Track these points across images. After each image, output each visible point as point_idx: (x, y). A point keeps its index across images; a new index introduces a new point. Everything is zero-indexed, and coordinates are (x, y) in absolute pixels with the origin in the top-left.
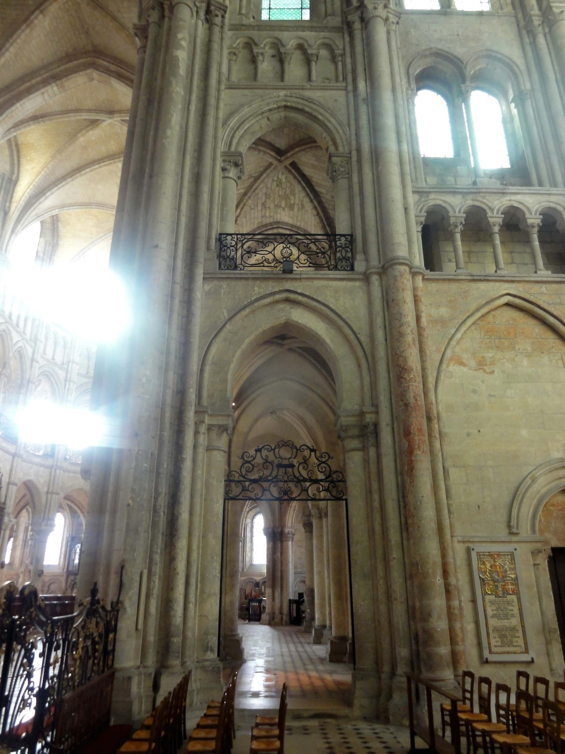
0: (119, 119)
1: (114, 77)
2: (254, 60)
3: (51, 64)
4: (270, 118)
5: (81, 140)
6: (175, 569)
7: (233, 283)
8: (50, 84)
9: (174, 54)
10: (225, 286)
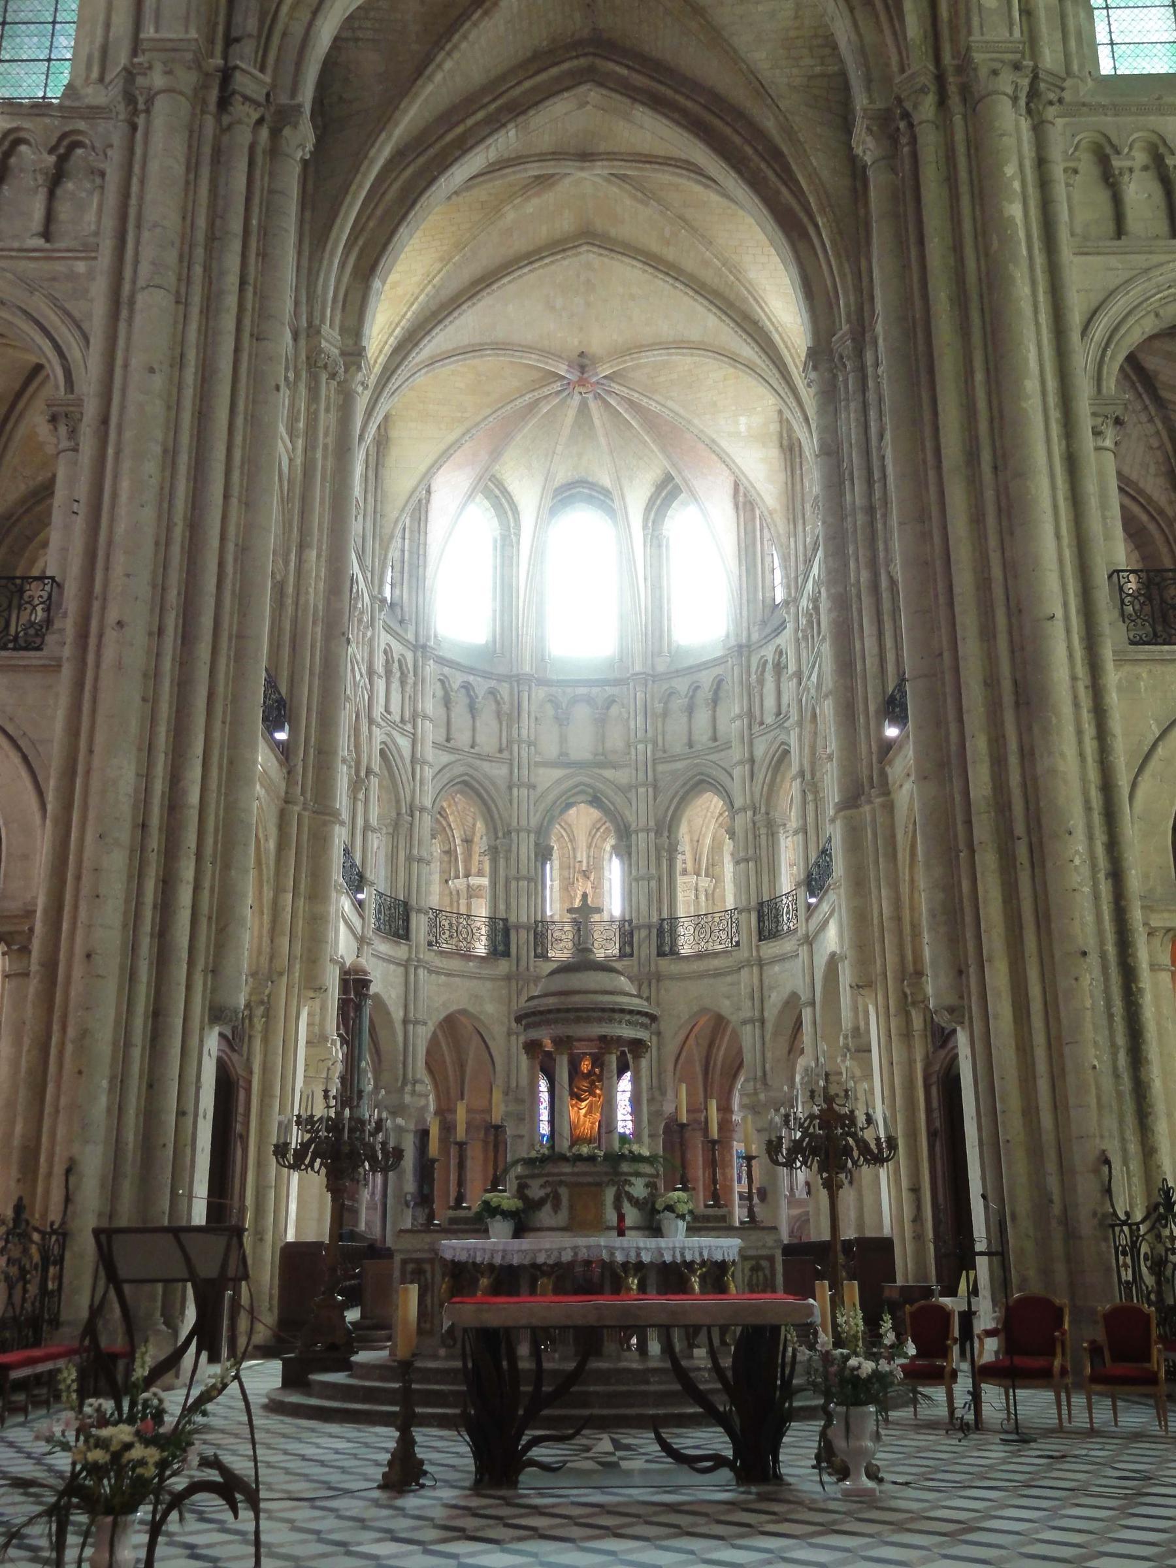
0: (606, 172)
1: (643, 103)
2: (1110, 181)
3: (503, 77)
4: (1161, 312)
5: (510, 215)
6: (1159, 1167)
7: (1158, 669)
8: (504, 125)
9: (1006, 215)
10: (1144, 675)
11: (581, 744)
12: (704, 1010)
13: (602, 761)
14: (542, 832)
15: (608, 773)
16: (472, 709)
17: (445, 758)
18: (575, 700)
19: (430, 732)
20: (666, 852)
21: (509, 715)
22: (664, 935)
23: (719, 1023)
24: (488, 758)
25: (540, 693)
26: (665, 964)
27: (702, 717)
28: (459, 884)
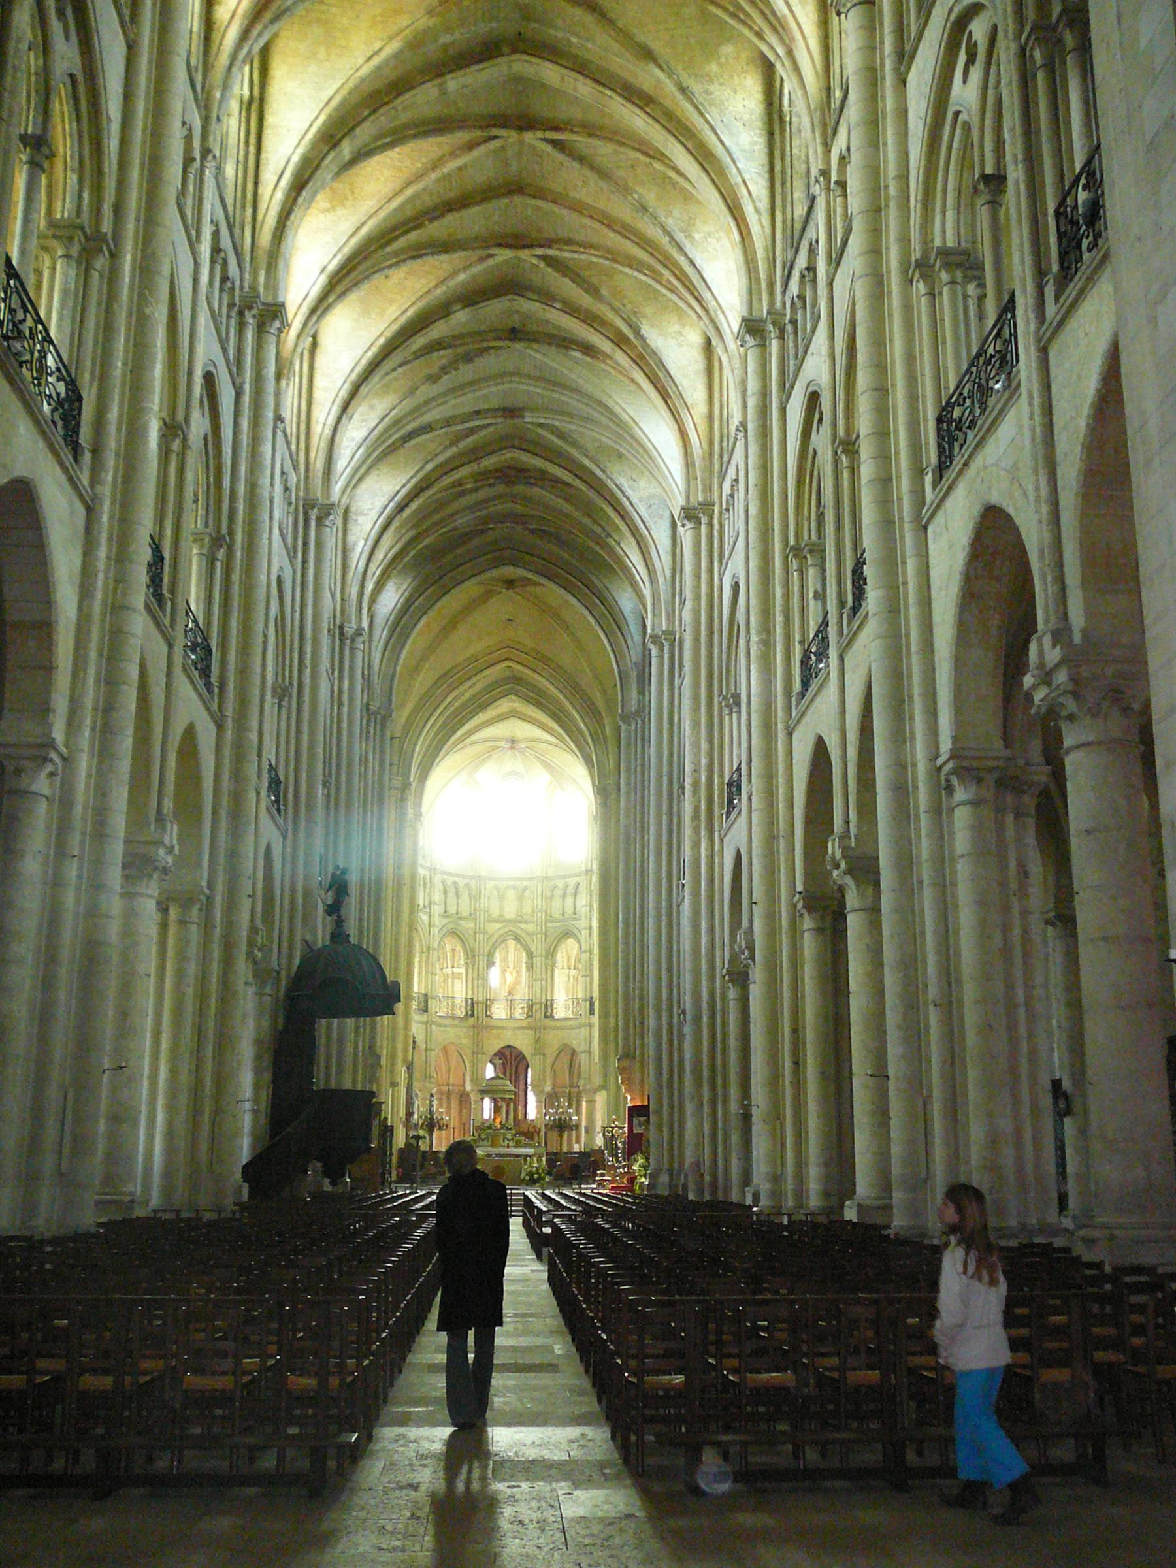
11: (510, 912)
12: (566, 1045)
13: (520, 920)
14: (490, 955)
15: (523, 926)
16: (457, 895)
17: (444, 921)
18: (507, 888)
19: (437, 910)
20: (550, 967)
21: (475, 897)
22: (548, 1006)
23: (574, 1052)
24: (465, 918)
25: (490, 885)
26: (548, 1022)
27: (569, 900)
28: (449, 971)
